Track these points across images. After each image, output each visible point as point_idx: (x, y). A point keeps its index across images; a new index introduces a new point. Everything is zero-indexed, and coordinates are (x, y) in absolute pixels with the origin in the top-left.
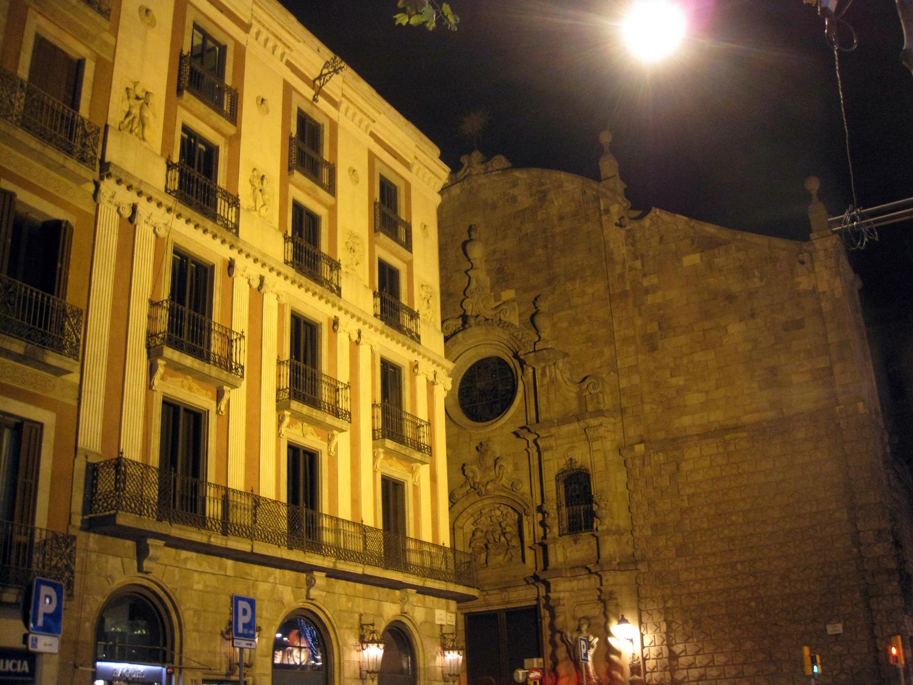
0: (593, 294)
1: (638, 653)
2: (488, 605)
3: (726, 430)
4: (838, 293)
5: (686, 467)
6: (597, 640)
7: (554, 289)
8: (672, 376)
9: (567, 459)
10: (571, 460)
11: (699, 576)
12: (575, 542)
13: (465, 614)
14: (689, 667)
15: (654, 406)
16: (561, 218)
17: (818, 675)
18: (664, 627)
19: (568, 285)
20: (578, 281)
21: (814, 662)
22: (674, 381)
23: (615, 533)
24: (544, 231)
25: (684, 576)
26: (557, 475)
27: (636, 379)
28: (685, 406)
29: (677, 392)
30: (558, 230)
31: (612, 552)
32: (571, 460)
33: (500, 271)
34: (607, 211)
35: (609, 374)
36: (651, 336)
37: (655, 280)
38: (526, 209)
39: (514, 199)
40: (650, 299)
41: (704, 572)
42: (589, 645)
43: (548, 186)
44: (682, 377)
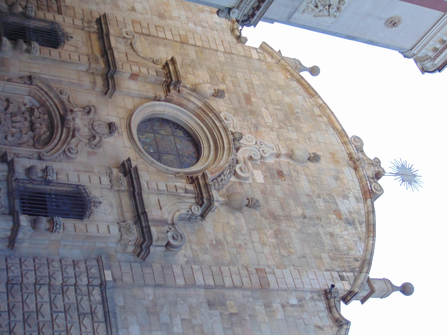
0: (263, 253)
7: (266, 218)
8: (182, 320)
9: (101, 199)
10: (100, 203)
15: (151, 298)
16: (331, 235)
19: (271, 231)
20: (274, 240)
22: (177, 321)
24: (319, 218)
27: (180, 282)
28: (151, 331)
29: (165, 324)
30: (321, 230)
32: (100, 203)
33: (280, 174)
34: (342, 278)
35: (185, 256)
36: (223, 304)
37: (280, 315)
38: (338, 205)
39: (346, 197)
40: (259, 308)
43: (359, 229)
44: (181, 331)
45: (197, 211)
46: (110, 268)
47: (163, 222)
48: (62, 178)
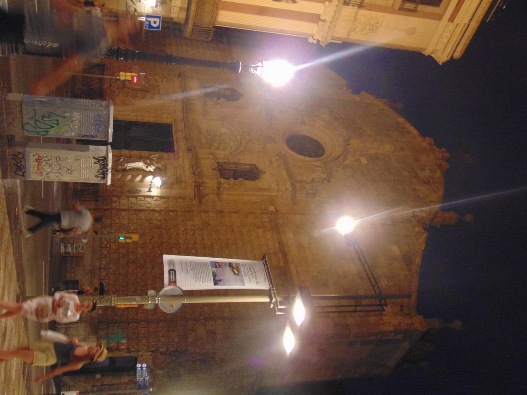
1: (142, 194)
2: (176, 132)
3: (285, 255)
4: (383, 328)
5: (260, 231)
6: (152, 171)
10: (265, 172)
11: (188, 231)
12: (214, 169)
13: (171, 125)
14: (129, 219)
17: (119, 238)
18: (157, 209)
21: (126, 238)
23: (219, 189)
25: (190, 223)
26: (255, 165)
31: (207, 185)
32: (265, 172)
39: (423, 170)
41: (191, 233)
42: (148, 165)
45: (324, 176)
46: (273, 205)
47: (302, 182)
48: (243, 162)
